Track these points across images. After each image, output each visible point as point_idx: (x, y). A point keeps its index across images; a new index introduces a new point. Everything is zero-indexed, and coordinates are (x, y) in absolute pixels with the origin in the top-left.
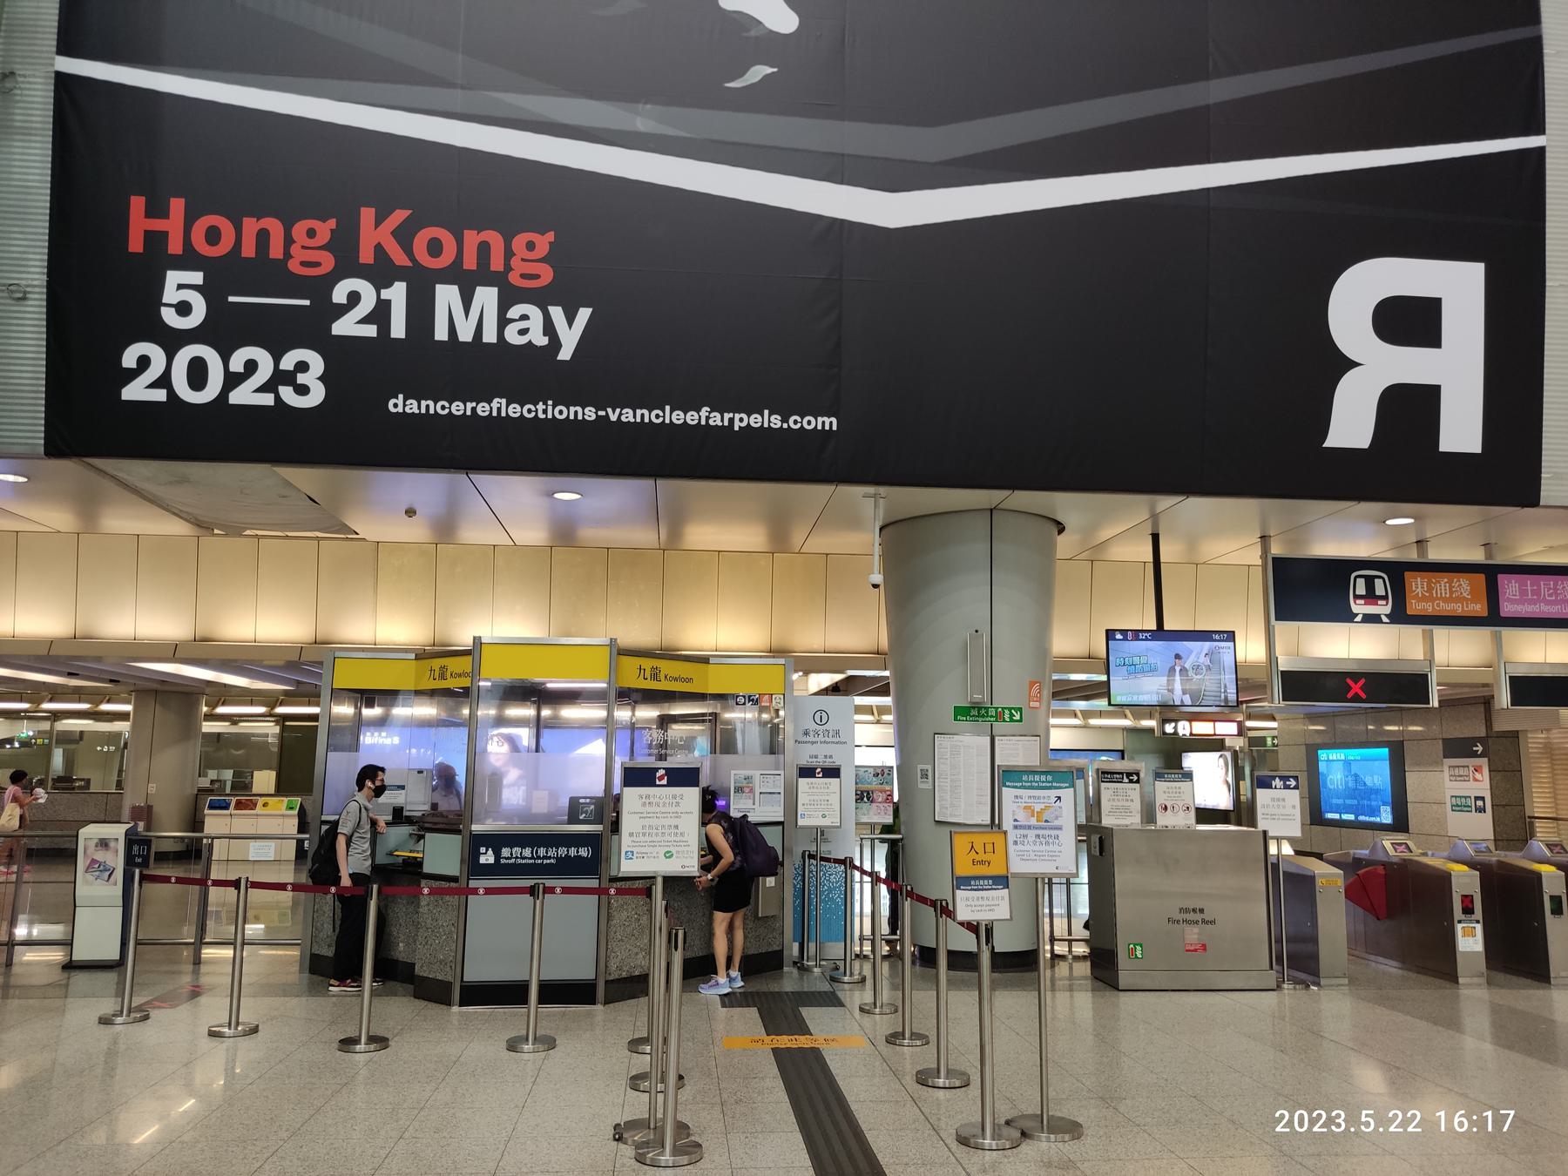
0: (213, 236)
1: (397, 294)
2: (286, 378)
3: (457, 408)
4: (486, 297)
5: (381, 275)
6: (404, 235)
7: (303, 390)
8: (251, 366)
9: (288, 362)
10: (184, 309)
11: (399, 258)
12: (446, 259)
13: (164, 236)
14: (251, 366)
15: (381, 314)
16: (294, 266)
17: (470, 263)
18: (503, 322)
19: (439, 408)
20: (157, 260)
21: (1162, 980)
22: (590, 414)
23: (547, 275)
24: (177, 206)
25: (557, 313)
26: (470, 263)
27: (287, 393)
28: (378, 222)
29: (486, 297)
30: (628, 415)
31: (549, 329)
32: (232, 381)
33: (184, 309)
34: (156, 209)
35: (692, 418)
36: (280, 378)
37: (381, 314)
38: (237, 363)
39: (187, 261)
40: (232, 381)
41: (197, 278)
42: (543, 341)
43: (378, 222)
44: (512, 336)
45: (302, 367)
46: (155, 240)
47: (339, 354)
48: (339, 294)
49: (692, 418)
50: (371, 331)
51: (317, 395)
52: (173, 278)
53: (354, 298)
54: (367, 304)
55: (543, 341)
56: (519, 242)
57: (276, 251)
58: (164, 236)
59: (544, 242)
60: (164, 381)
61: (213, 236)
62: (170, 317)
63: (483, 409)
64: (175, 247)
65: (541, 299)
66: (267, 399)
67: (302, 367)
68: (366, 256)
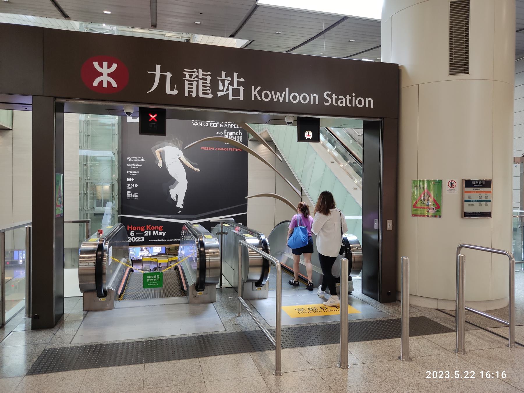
0: (134, 228)
1: (150, 232)
2: (141, 239)
3: (155, 240)
4: (157, 232)
5: (148, 230)
6: (150, 227)
7: (142, 240)
8: (138, 238)
9: (141, 238)
10: (132, 234)
11: (150, 229)
12: (154, 229)
13: (129, 227)
14: (138, 238)
15: (148, 234)
16: (141, 230)
17: (156, 229)
18: (158, 233)
19: (153, 241)
20: (130, 230)
21: (278, 295)
22: (166, 240)
23: (162, 229)
24: (131, 226)
25: (163, 232)
26: (156, 229)
27: (141, 240)
28: (148, 226)
29: (157, 232)
30: (169, 240)
31: (162, 234)
32: (136, 240)
33: (132, 234)
34: (130, 227)
35: (174, 240)
36: (140, 239)
37: (148, 234)
38: (137, 238)
39: (133, 230)
40: (136, 240)
41: (133, 232)
42: (162, 235)
43: (148, 226)
44: (159, 235)
45: (142, 238)
46: (130, 229)
47: (145, 237)
48: (145, 232)
49: (174, 240)
50: (148, 235)
51: (143, 240)
52: (131, 232)
53: (146, 232)
54: (147, 233)
55: (162, 235)
56: (160, 227)
57: (140, 229)
58: (129, 227)
59: (162, 227)
60: (131, 240)
61: (134, 228)
62: (131, 235)
63: (157, 240)
64: (131, 229)
65: (162, 231)
66: (139, 241)
67: (142, 238)
68: (147, 229)
